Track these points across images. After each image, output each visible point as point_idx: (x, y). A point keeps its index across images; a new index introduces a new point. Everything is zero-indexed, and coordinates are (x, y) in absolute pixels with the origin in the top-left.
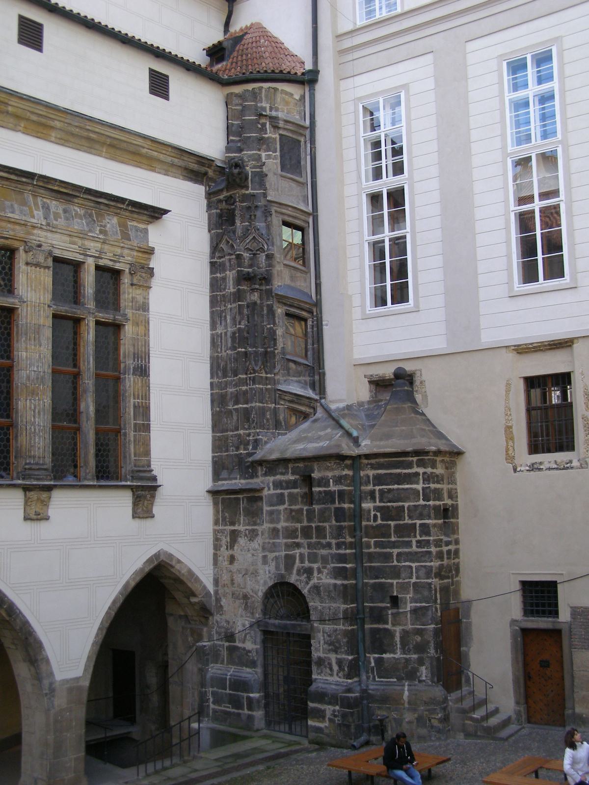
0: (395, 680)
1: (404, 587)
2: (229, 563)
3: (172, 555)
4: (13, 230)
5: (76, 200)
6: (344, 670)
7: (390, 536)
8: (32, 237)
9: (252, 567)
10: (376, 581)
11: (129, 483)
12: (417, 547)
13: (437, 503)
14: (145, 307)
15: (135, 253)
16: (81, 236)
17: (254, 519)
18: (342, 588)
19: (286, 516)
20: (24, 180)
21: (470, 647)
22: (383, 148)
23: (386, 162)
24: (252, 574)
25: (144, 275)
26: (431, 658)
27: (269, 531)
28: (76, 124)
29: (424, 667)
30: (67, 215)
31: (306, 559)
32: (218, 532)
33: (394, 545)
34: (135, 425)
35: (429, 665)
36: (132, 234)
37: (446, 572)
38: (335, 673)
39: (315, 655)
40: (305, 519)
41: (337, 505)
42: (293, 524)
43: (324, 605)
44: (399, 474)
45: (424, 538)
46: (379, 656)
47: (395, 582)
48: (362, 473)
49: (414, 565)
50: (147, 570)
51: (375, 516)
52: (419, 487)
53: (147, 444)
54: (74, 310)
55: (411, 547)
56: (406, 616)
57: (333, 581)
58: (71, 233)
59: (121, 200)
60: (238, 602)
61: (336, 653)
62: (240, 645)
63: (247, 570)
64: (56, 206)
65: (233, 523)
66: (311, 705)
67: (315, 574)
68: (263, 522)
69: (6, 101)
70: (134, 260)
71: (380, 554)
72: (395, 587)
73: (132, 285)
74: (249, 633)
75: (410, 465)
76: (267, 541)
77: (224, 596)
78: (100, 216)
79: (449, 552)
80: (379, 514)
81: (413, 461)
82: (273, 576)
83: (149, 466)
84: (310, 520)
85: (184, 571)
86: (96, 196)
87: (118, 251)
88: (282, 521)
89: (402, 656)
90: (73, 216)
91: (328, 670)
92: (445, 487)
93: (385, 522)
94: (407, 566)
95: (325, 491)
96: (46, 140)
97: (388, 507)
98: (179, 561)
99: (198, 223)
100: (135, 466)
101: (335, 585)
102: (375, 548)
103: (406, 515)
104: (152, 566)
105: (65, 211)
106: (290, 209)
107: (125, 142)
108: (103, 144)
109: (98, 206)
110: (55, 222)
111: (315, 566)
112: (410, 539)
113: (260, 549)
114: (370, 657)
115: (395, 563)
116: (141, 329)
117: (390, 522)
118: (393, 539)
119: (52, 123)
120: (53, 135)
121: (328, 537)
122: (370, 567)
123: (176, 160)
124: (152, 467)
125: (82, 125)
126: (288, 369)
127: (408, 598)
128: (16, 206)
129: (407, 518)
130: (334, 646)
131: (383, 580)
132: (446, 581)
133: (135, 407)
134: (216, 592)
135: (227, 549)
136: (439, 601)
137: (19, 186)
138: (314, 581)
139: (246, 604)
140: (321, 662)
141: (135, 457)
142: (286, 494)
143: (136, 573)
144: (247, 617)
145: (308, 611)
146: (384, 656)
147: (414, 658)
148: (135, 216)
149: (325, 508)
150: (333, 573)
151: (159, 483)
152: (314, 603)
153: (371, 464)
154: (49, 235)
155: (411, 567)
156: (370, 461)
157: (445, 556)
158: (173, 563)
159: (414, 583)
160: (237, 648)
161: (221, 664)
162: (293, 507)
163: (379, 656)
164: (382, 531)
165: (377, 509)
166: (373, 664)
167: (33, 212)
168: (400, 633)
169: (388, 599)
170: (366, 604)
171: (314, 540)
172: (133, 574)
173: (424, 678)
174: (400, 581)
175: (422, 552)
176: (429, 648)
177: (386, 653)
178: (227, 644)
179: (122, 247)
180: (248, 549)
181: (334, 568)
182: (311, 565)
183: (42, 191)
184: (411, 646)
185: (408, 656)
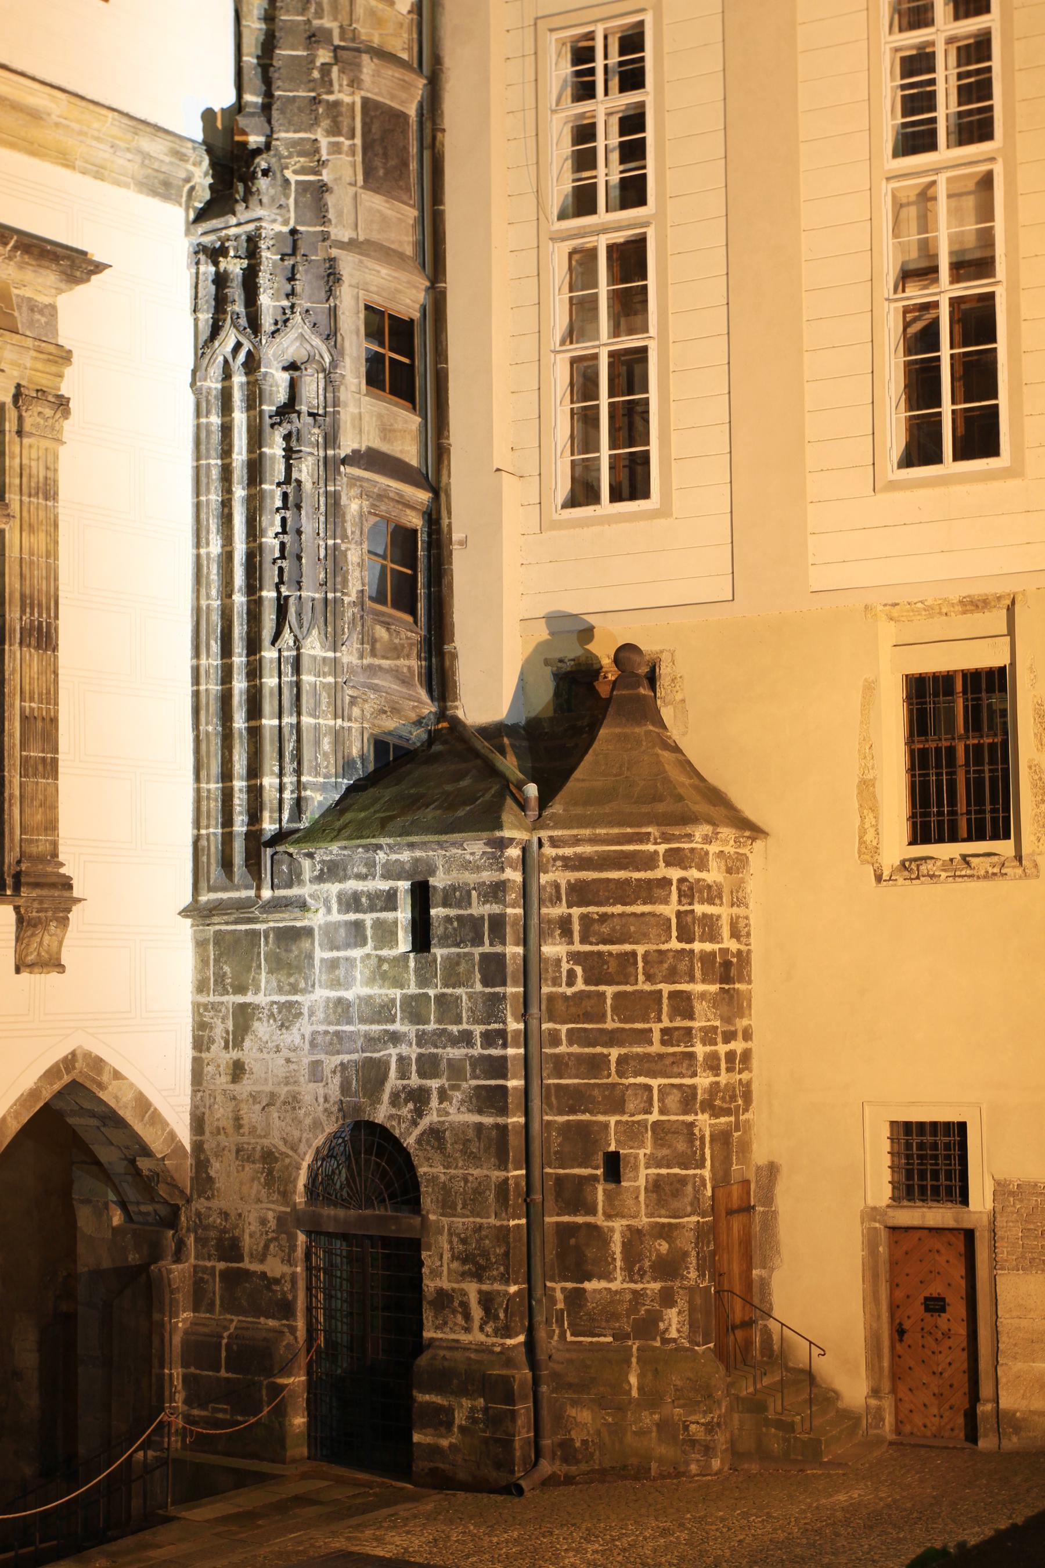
0: (610, 1339)
1: (632, 1133)
2: (229, 1078)
3: (101, 1060)
6: (496, 1317)
7: (602, 1018)
9: (286, 1089)
10: (571, 1118)
12: (663, 1043)
13: (708, 947)
17: (292, 980)
18: (494, 1133)
19: (367, 971)
21: (772, 1269)
22: (600, 144)
23: (608, 173)
24: (285, 1103)
26: (691, 1290)
27: (327, 1006)
29: (675, 1310)
31: (414, 1068)
32: (206, 1010)
33: (612, 1038)
34: (25, 761)
35: (686, 1306)
37: (723, 1099)
38: (476, 1324)
39: (430, 1285)
40: (413, 978)
41: (487, 948)
42: (383, 991)
43: (453, 1171)
44: (627, 881)
45: (679, 1023)
46: (575, 1285)
47: (613, 1120)
48: (544, 878)
49: (655, 1083)
51: (571, 974)
53: (50, 805)
55: (651, 1043)
56: (637, 1197)
57: (476, 1118)
60: (249, 1168)
61: (480, 1280)
62: (255, 1267)
63: (272, 1095)
65: (241, 989)
66: (423, 1398)
67: (434, 1102)
68: (313, 986)
71: (579, 1058)
74: (276, 1239)
75: (649, 861)
76: (322, 1028)
77: (217, 1156)
79: (730, 1056)
80: (579, 970)
81: (656, 852)
82: (335, 1109)
83: (55, 855)
84: (423, 982)
85: (128, 1097)
88: (358, 983)
89: (626, 1285)
91: (460, 1319)
92: (723, 911)
93: (593, 988)
94: (640, 1085)
95: (459, 918)
97: (600, 954)
98: (117, 1075)
101: (479, 1127)
102: (570, 1043)
103: (640, 970)
104: (57, 1086)
111: (434, 1084)
112: (646, 1026)
113: (307, 1046)
114: (554, 1289)
115: (614, 1079)
116: (40, 541)
117: (602, 988)
118: (610, 1025)
121: (465, 1019)
122: (558, 1086)
124: (62, 858)
127: (641, 1156)
129: (641, 978)
130: (475, 1263)
131: (586, 1117)
132: (723, 1120)
133: (25, 719)
134: (198, 1147)
135: (226, 1047)
138: (431, 1118)
139: (270, 1173)
140: (444, 1300)
142: (369, 923)
144: (273, 1202)
145: (417, 1186)
146: (587, 1285)
147: (653, 1290)
149: (458, 954)
150: (474, 1100)
151: (76, 893)
152: (429, 1169)
153: (564, 859)
155: (648, 1088)
156: (561, 852)
157: (723, 1065)
158: (105, 1078)
159: (655, 1123)
160: (247, 1274)
161: (208, 1311)
162: (385, 953)
163: (575, 1285)
164: (584, 1008)
165: (575, 957)
166: (560, 1305)
168: (622, 1232)
169: (600, 1158)
170: (548, 1170)
171: (432, 1026)
172: (15, 1104)
173: (674, 1334)
174: (625, 1118)
175: (674, 1054)
176: (688, 1268)
177: (589, 1280)
178: (221, 1265)
180: (277, 1046)
181: (478, 1087)
182: (424, 1082)
184: (647, 1264)
185: (639, 1286)
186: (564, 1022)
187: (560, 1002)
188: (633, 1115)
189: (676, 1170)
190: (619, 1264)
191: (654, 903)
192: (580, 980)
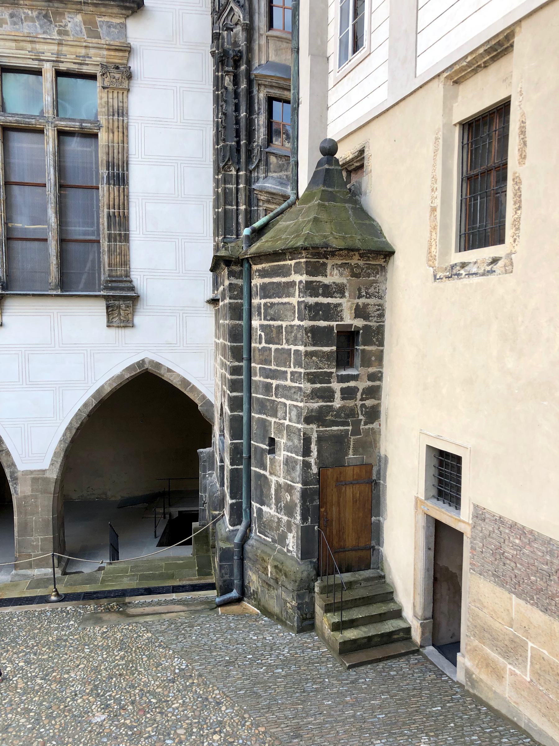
0: (270, 540)
11: (102, 293)
14: (121, 112)
15: (105, 53)
16: (28, 39)
25: (117, 76)
30: (14, 19)
34: (110, 235)
36: (102, 31)
44: (279, 284)
47: (273, 420)
50: (127, 376)
51: (260, 335)
58: (16, 38)
70: (105, 60)
72: (273, 427)
73: (104, 88)
75: (285, 271)
78: (59, 14)
87: (83, 51)
90: (22, 20)
97: (270, 326)
98: (169, 370)
99: (198, 8)
100: (109, 276)
103: (284, 338)
105: (12, 16)
115: (274, 398)
117: (271, 346)
118: (273, 367)
124: (132, 277)
126: (267, 164)
133: (109, 216)
136: (315, 453)
143: (113, 379)
148: (103, 9)
155: (285, 405)
158: (162, 372)
172: (109, 380)
174: (277, 420)
175: (295, 387)
179: (86, 47)
184: (283, 505)
185: (280, 516)
186: (258, 364)
187: (257, 352)
188: (280, 420)
189: (294, 455)
190: (273, 500)
191: (289, 297)
192: (263, 341)
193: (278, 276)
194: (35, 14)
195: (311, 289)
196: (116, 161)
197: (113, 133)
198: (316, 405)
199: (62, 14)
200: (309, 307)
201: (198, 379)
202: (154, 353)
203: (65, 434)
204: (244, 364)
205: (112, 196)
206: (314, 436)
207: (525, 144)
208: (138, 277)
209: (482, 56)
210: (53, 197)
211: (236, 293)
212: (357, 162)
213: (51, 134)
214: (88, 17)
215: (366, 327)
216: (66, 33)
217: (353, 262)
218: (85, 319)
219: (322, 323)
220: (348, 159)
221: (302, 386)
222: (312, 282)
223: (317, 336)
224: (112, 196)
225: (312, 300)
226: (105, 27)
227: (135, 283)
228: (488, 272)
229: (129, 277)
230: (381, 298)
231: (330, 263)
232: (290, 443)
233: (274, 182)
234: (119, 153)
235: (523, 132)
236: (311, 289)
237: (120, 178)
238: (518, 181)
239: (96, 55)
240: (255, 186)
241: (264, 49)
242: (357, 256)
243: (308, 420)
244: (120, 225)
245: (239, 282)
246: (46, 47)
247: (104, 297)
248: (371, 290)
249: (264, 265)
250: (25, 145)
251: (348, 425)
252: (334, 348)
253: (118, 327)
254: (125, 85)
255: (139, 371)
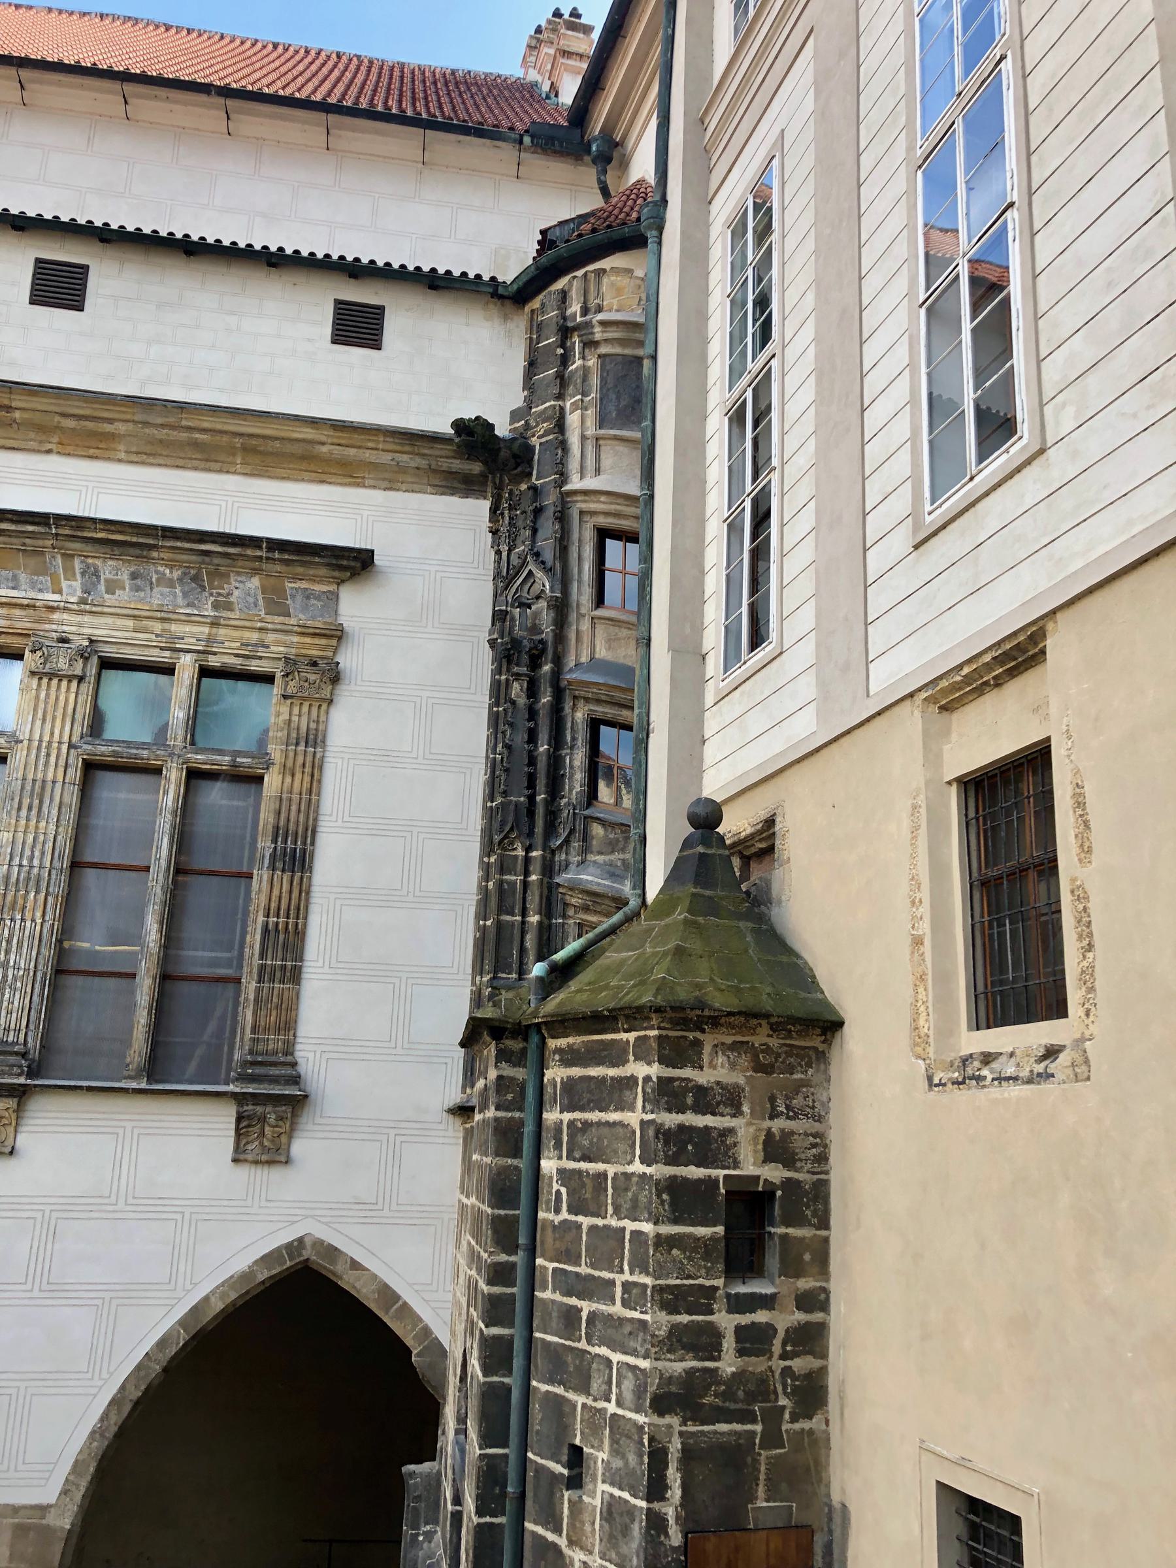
4: (7, 618)
5: (155, 554)
8: (47, 626)
11: (231, 1088)
14: (314, 739)
15: (296, 639)
16: (159, 615)
20: (30, 528)
25: (312, 677)
28: (160, 421)
30: (138, 581)
34: (262, 968)
44: (602, 1080)
47: (580, 1400)
52: (633, 1118)
54: (134, 751)
58: (136, 613)
59: (254, 542)
64: (108, 569)
69: (6, 402)
70: (294, 651)
72: (579, 1418)
73: (285, 697)
75: (616, 1055)
86: (194, 542)
87: (255, 636)
90: (152, 584)
96: (109, 459)
98: (355, 1265)
99: (471, 571)
100: (251, 1052)
103: (609, 1201)
105: (134, 576)
106: (603, 499)
107: (277, 439)
108: (232, 451)
109: (207, 559)
110: (107, 596)
115: (583, 1345)
118: (584, 1270)
119: (108, 428)
120: (122, 447)
123: (405, 457)
124: (298, 1054)
125: (171, 420)
126: (586, 837)
128: (23, 577)
133: (266, 930)
136: (675, 1493)
137: (27, 541)
141: (254, 1031)
143: (230, 1282)
148: (300, 570)
154: (87, 619)
155: (609, 1362)
158: (339, 1268)
167: (60, 583)
172: (223, 1284)
174: (589, 1402)
175: (632, 1320)
179: (261, 629)
183: (77, 545)
186: (551, 1261)
187: (549, 1232)
188: (595, 1400)
189: (626, 1495)
191: (622, 1110)
192: (564, 1206)
193: (600, 1063)
194: (177, 574)
195: (668, 1094)
196: (292, 826)
197: (293, 775)
198: (678, 1367)
199: (225, 576)
200: (666, 1135)
201: (415, 1287)
202: (326, 1224)
203: (105, 1417)
204: (518, 1258)
205: (276, 892)
206: (675, 1446)
207: (1086, 824)
208: (311, 1056)
209: (988, 667)
210: (159, 891)
211: (510, 1096)
212: (760, 841)
213: (174, 775)
214: (272, 581)
215: (788, 1183)
216: (229, 607)
217: (757, 1040)
218: (189, 1142)
219: (694, 1172)
220: (743, 834)
221: (647, 1317)
222: (671, 1080)
223: (682, 1200)
224: (276, 892)
225: (670, 1120)
226: (299, 598)
227: (302, 1069)
228: (1039, 1075)
229: (292, 1054)
230: (819, 1119)
231: (709, 1040)
232: (618, 1463)
233: (599, 871)
234: (299, 811)
235: (1080, 803)
236: (668, 1094)
237: (295, 858)
238: (1081, 896)
239: (278, 643)
240: (562, 878)
241: (586, 639)
242: (765, 1029)
243: (660, 1405)
244: (285, 948)
245: (519, 1073)
246: (188, 628)
247: (234, 1095)
248: (797, 1102)
249: (571, 1040)
250: (122, 795)
251: (754, 1421)
252: (720, 1230)
253: (256, 1162)
254: (326, 692)
255: (288, 1264)
